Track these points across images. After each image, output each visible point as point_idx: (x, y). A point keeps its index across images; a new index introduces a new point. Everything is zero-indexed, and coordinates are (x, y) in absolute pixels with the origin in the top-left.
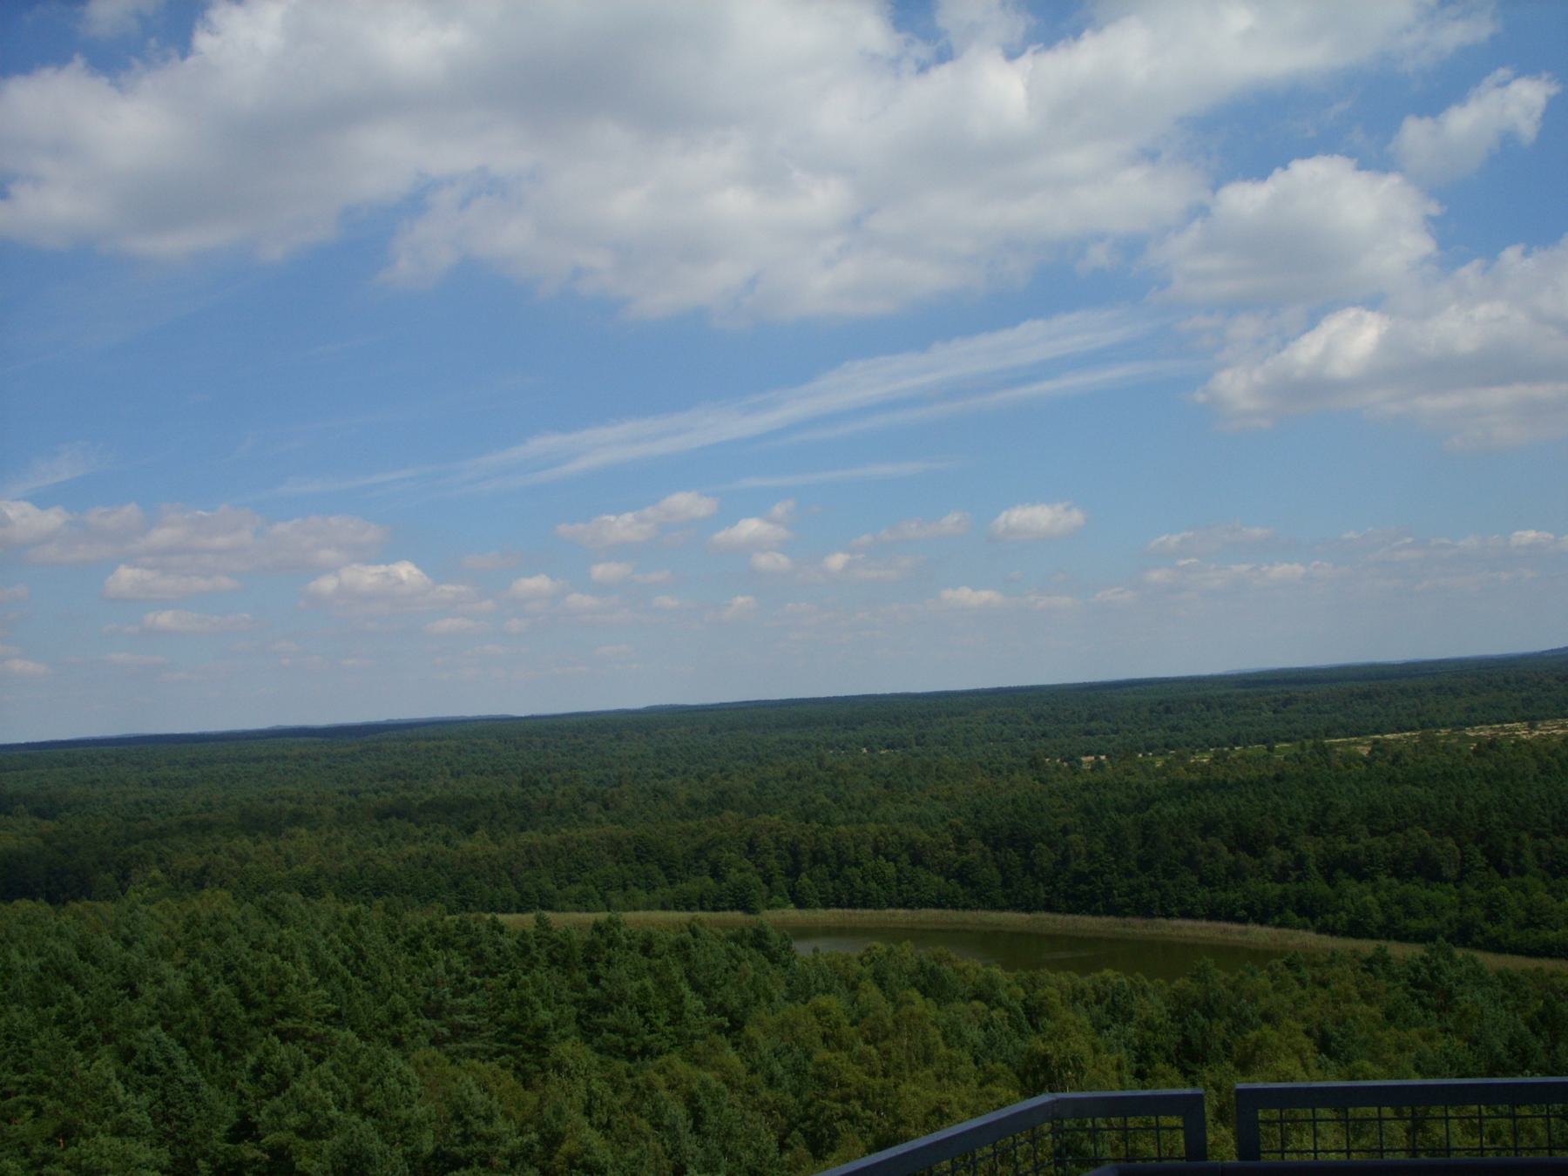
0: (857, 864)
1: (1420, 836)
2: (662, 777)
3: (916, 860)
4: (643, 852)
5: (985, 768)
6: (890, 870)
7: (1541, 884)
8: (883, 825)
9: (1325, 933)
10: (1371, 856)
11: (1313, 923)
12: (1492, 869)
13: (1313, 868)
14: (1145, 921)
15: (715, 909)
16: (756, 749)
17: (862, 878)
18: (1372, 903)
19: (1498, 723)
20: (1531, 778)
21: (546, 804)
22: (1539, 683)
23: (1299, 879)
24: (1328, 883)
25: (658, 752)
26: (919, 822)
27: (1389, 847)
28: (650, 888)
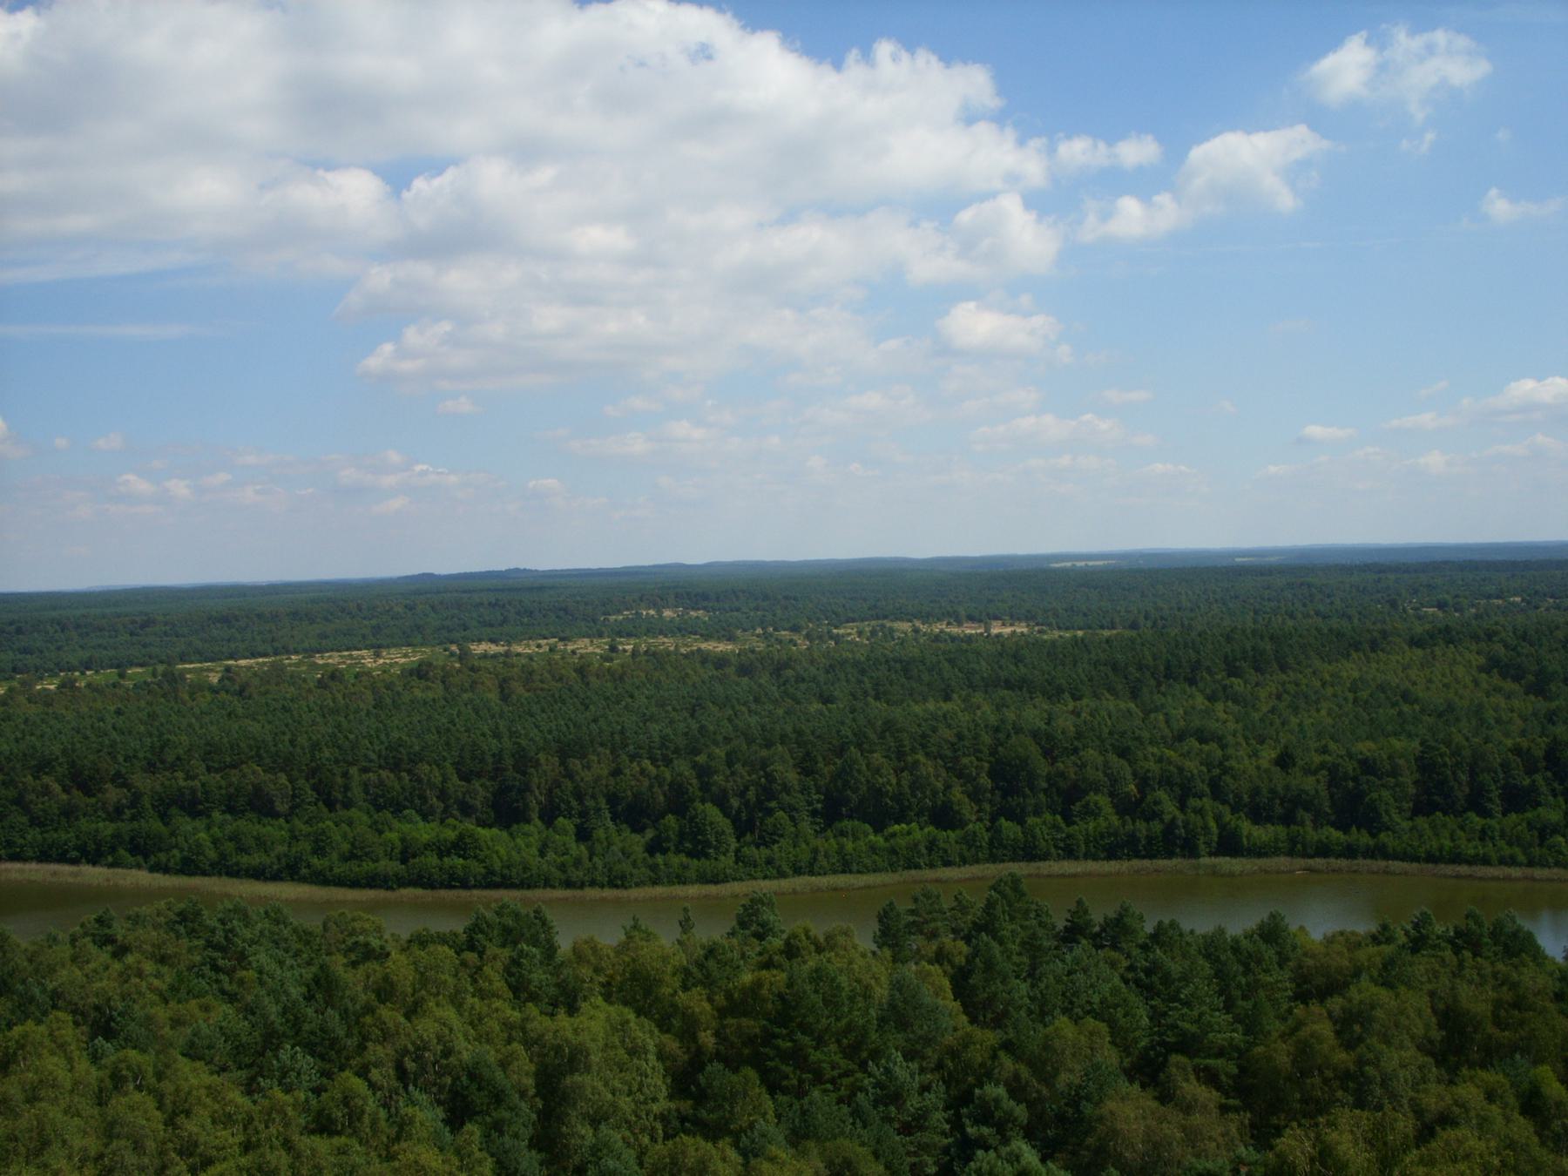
1: (254, 772)
7: (365, 818)
9: (157, 871)
10: (206, 793)
11: (146, 863)
12: (320, 804)
13: (148, 806)
18: (205, 840)
19: (347, 650)
20: (363, 713)
22: (388, 611)
23: (133, 818)
24: (162, 820)
27: (223, 783)
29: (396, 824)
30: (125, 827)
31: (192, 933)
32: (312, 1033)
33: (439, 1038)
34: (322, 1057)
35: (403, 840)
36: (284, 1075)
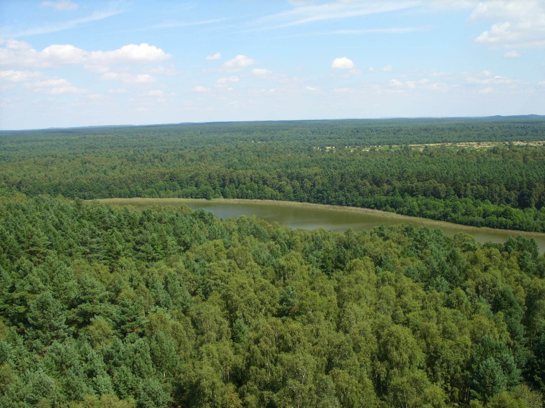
0: (245, 184)
1: (434, 183)
2: (182, 150)
3: (265, 183)
4: (172, 178)
5: (293, 150)
6: (256, 186)
7: (471, 201)
8: (254, 171)
10: (417, 189)
12: (456, 195)
14: (340, 207)
15: (196, 198)
16: (215, 140)
17: (246, 189)
20: (473, 165)
21: (141, 159)
23: (392, 195)
24: (402, 196)
25: (182, 141)
26: (266, 170)
27: (423, 186)
28: (174, 190)
29: (482, 204)
30: (390, 198)
31: (409, 235)
32: (447, 273)
33: (492, 280)
34: (450, 282)
35: (484, 210)
36: (438, 286)
